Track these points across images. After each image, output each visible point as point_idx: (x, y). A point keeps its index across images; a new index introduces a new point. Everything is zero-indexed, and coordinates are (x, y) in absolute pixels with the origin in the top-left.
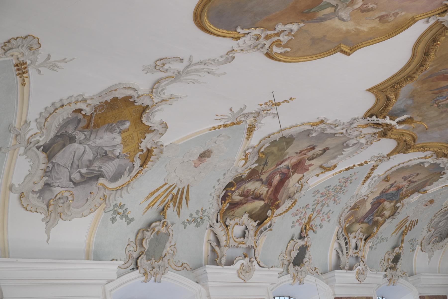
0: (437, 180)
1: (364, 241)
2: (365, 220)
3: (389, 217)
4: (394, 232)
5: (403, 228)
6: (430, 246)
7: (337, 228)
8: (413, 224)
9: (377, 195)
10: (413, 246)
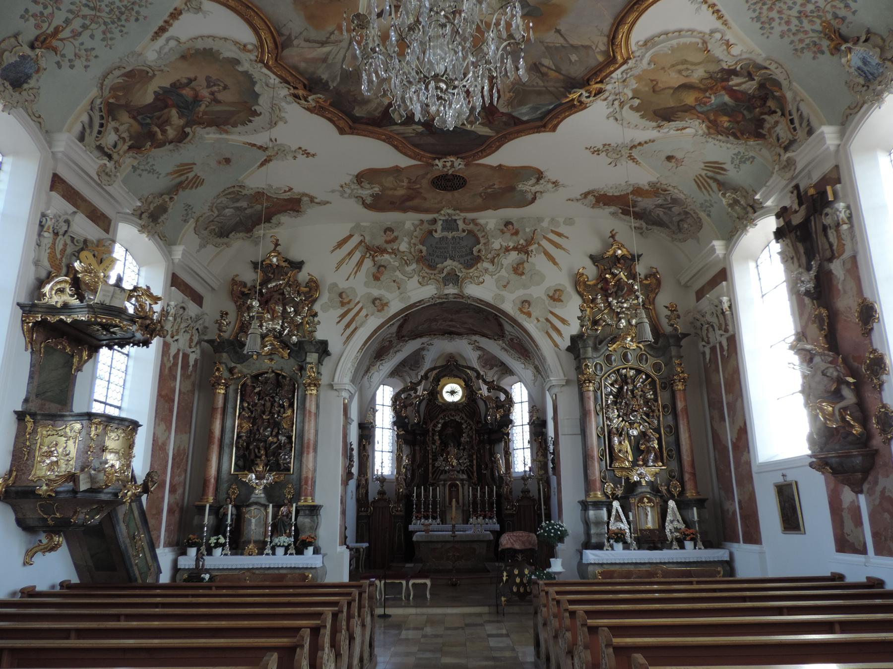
0: (243, 124)
1: (127, 148)
2: (139, 118)
3: (171, 142)
4: (171, 174)
5: (183, 178)
6: (206, 233)
7: (94, 92)
8: (197, 182)
9: (166, 84)
10: (187, 215)
